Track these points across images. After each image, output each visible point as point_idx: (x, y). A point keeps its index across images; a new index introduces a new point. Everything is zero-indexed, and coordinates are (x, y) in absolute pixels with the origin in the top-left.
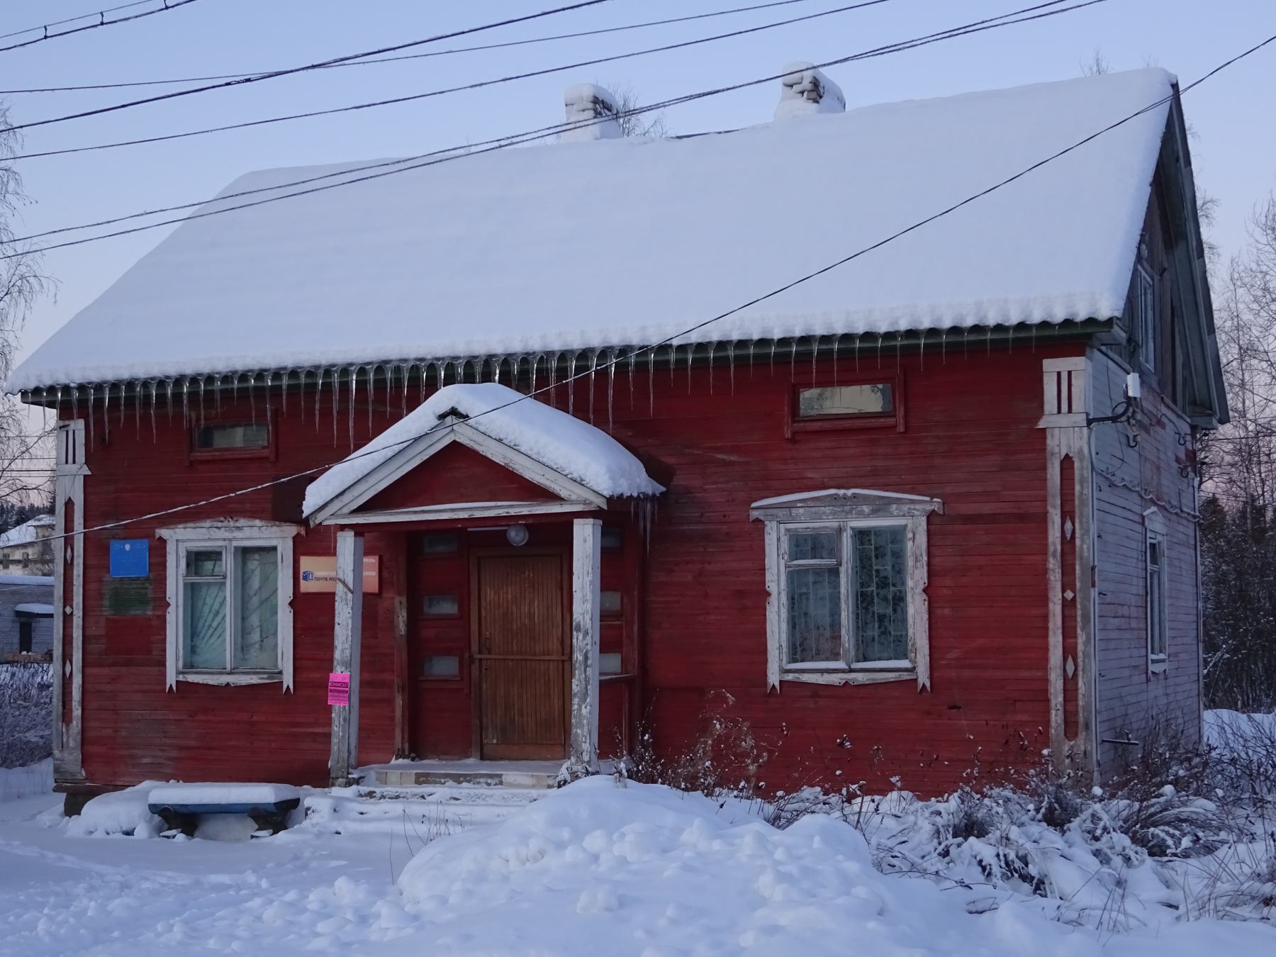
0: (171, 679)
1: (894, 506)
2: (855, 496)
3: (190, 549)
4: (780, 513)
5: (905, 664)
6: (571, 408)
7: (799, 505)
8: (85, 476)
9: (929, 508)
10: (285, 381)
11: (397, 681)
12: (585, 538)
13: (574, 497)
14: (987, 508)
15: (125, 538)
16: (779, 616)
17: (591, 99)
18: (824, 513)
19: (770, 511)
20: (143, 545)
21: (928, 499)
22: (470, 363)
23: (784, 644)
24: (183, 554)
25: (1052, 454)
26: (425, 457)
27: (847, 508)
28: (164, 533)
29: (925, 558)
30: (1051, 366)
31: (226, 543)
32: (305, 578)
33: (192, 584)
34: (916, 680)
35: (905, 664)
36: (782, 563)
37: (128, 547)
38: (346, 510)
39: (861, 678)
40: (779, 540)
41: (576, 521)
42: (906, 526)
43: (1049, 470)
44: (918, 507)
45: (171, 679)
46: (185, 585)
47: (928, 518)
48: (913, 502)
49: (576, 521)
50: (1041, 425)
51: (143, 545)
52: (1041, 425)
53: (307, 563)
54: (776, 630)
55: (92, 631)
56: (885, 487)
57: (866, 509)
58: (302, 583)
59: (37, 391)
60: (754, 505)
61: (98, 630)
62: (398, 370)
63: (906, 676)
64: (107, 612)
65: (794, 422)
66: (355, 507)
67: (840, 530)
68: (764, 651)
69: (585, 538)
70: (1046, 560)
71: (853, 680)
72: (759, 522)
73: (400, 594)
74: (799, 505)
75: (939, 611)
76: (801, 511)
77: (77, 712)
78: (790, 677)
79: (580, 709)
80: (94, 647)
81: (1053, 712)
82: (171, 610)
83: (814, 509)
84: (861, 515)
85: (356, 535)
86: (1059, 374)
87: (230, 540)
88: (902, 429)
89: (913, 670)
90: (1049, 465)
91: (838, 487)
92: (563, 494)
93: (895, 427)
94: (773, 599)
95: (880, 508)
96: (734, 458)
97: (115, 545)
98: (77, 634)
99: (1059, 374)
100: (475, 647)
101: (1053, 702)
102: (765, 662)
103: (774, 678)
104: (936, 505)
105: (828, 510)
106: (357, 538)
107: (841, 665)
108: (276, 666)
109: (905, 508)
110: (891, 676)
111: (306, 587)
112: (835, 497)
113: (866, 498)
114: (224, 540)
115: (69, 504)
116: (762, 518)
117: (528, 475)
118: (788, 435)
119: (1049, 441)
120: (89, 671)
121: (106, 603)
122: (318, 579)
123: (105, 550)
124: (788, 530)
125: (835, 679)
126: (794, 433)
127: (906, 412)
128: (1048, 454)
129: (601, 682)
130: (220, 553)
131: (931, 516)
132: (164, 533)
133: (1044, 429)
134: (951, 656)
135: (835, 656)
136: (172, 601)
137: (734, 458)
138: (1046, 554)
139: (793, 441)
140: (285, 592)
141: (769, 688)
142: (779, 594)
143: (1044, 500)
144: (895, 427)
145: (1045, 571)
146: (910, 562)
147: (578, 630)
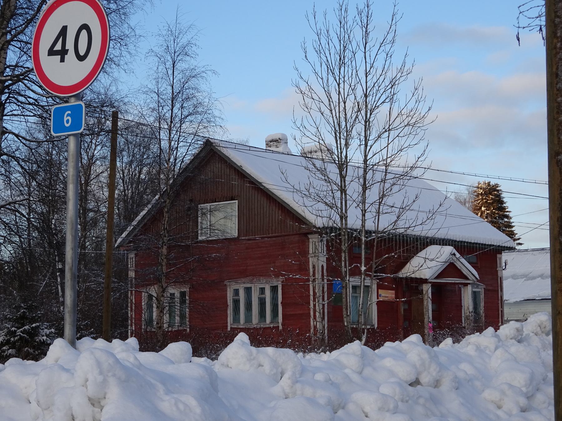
13: (471, 279)
22: (443, 240)
24: (351, 286)
30: (498, 256)
32: (380, 296)
38: (433, 278)
42: (480, 291)
44: (482, 287)
48: (482, 285)
49: (469, 285)
53: (381, 291)
57: (475, 286)
88: (479, 267)
92: (470, 278)
93: (478, 267)
100: (412, 319)
104: (485, 287)
108: (372, 323)
109: (481, 287)
115: (322, 266)
117: (464, 272)
119: (499, 273)
122: (383, 296)
131: (484, 289)
140: (375, 299)
143: (498, 287)
144: (478, 267)
145: (498, 303)
146: (481, 300)
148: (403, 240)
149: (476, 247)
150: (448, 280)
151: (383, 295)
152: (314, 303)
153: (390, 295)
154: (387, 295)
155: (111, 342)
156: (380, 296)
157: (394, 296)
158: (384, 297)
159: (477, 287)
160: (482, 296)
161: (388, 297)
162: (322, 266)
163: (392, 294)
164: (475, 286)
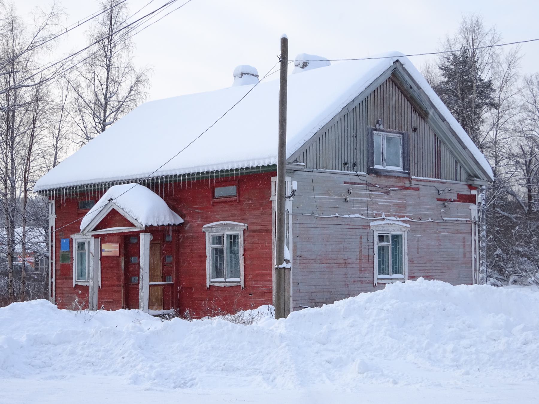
0: (74, 284)
1: (236, 227)
2: (227, 224)
3: (79, 242)
4: (209, 229)
5: (238, 279)
6: (159, 194)
7: (214, 227)
8: (55, 218)
9: (244, 228)
10: (78, 190)
11: (122, 284)
12: (145, 240)
13: (138, 226)
14: (258, 228)
15: (65, 238)
16: (209, 264)
17: (240, 74)
18: (220, 229)
19: (207, 229)
20: (68, 240)
21: (243, 224)
23: (211, 273)
24: (77, 243)
25: (273, 209)
26: (107, 213)
27: (225, 228)
28: (72, 236)
29: (243, 245)
31: (85, 240)
32: (103, 251)
33: (81, 253)
34: (241, 285)
35: (238, 279)
36: (210, 246)
37: (65, 241)
39: (228, 285)
40: (209, 238)
41: (141, 233)
43: (273, 214)
44: (241, 227)
45: (74, 284)
46: (78, 253)
47: (244, 231)
49: (141, 234)
50: (271, 200)
51: (68, 240)
52: (271, 200)
54: (208, 268)
55: (58, 268)
56: (234, 220)
57: (229, 228)
58: (102, 252)
59: (40, 191)
60: (204, 226)
61: (58, 268)
62: (148, 180)
63: (239, 284)
64: (61, 262)
65: (213, 199)
66: (92, 229)
67: (223, 235)
68: (206, 276)
69: (145, 240)
70: (271, 246)
71: (226, 285)
72: (204, 232)
73: (122, 256)
74: (214, 227)
75: (247, 262)
76: (214, 229)
77: (54, 294)
78: (212, 284)
79: (141, 294)
80: (58, 273)
81: (273, 296)
82: (74, 261)
83: (217, 228)
84: (228, 230)
85: (95, 238)
86: (275, 182)
87: (87, 239)
88: (238, 201)
89: (239, 282)
90: (273, 213)
91: (224, 220)
92: (136, 225)
94: (208, 258)
95: (233, 227)
96: (199, 211)
97: (62, 240)
98: (54, 269)
99: (275, 182)
101: (273, 293)
102: (206, 279)
103: (208, 285)
105: (220, 228)
106: (96, 239)
107: (222, 280)
109: (238, 228)
110: (235, 284)
111: (104, 254)
112: (222, 224)
113: (230, 225)
114: (86, 239)
115: (52, 227)
116: (205, 231)
118: (212, 204)
119: (273, 205)
120: (58, 281)
121: (60, 259)
122: (106, 251)
123: (60, 241)
124: (211, 235)
125: (222, 285)
126: (213, 203)
127: (239, 195)
128: (272, 209)
129: (150, 286)
130: (84, 243)
132: (72, 236)
133: (271, 201)
134: (249, 277)
135: (222, 276)
136: (74, 258)
137: (199, 211)
138: (271, 243)
139: (213, 205)
141: (207, 287)
142: (209, 256)
147: (141, 269)
148: (157, 183)
149: (180, 180)
150: (104, 231)
151: (106, 250)
152: (52, 261)
153: (113, 250)
154: (111, 250)
155: (425, 280)
156: (103, 251)
157: (118, 250)
158: (107, 251)
159: (231, 229)
160: (241, 240)
161: (111, 251)
162: (52, 227)
163: (115, 248)
164: (229, 228)
